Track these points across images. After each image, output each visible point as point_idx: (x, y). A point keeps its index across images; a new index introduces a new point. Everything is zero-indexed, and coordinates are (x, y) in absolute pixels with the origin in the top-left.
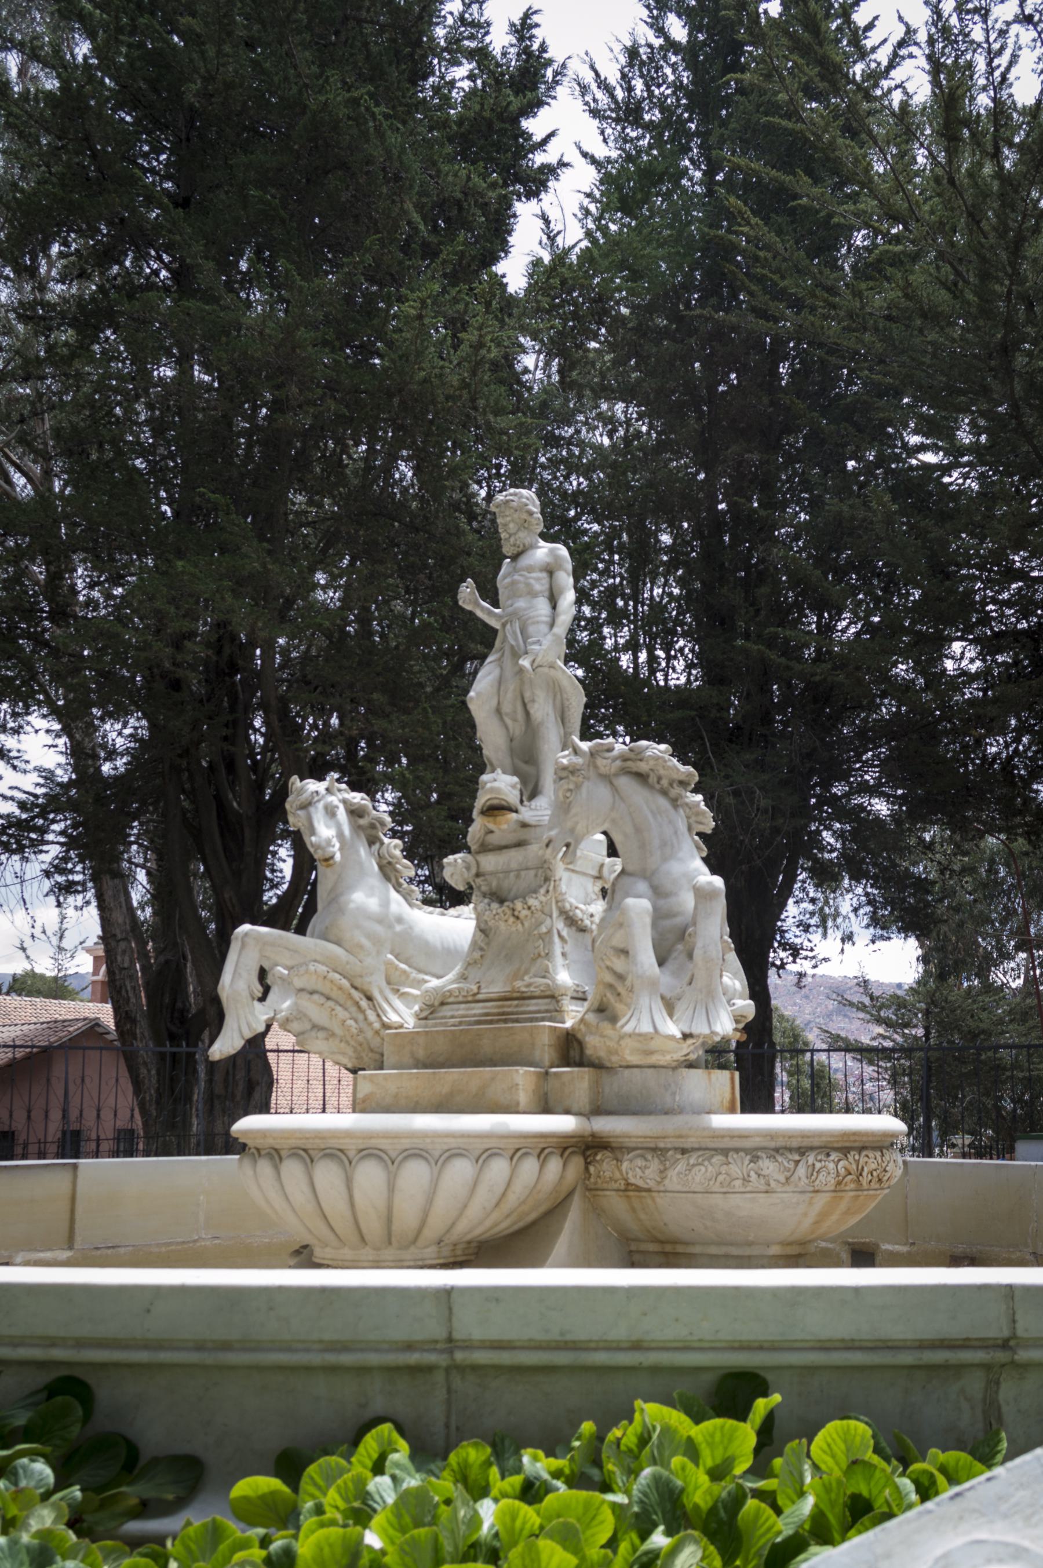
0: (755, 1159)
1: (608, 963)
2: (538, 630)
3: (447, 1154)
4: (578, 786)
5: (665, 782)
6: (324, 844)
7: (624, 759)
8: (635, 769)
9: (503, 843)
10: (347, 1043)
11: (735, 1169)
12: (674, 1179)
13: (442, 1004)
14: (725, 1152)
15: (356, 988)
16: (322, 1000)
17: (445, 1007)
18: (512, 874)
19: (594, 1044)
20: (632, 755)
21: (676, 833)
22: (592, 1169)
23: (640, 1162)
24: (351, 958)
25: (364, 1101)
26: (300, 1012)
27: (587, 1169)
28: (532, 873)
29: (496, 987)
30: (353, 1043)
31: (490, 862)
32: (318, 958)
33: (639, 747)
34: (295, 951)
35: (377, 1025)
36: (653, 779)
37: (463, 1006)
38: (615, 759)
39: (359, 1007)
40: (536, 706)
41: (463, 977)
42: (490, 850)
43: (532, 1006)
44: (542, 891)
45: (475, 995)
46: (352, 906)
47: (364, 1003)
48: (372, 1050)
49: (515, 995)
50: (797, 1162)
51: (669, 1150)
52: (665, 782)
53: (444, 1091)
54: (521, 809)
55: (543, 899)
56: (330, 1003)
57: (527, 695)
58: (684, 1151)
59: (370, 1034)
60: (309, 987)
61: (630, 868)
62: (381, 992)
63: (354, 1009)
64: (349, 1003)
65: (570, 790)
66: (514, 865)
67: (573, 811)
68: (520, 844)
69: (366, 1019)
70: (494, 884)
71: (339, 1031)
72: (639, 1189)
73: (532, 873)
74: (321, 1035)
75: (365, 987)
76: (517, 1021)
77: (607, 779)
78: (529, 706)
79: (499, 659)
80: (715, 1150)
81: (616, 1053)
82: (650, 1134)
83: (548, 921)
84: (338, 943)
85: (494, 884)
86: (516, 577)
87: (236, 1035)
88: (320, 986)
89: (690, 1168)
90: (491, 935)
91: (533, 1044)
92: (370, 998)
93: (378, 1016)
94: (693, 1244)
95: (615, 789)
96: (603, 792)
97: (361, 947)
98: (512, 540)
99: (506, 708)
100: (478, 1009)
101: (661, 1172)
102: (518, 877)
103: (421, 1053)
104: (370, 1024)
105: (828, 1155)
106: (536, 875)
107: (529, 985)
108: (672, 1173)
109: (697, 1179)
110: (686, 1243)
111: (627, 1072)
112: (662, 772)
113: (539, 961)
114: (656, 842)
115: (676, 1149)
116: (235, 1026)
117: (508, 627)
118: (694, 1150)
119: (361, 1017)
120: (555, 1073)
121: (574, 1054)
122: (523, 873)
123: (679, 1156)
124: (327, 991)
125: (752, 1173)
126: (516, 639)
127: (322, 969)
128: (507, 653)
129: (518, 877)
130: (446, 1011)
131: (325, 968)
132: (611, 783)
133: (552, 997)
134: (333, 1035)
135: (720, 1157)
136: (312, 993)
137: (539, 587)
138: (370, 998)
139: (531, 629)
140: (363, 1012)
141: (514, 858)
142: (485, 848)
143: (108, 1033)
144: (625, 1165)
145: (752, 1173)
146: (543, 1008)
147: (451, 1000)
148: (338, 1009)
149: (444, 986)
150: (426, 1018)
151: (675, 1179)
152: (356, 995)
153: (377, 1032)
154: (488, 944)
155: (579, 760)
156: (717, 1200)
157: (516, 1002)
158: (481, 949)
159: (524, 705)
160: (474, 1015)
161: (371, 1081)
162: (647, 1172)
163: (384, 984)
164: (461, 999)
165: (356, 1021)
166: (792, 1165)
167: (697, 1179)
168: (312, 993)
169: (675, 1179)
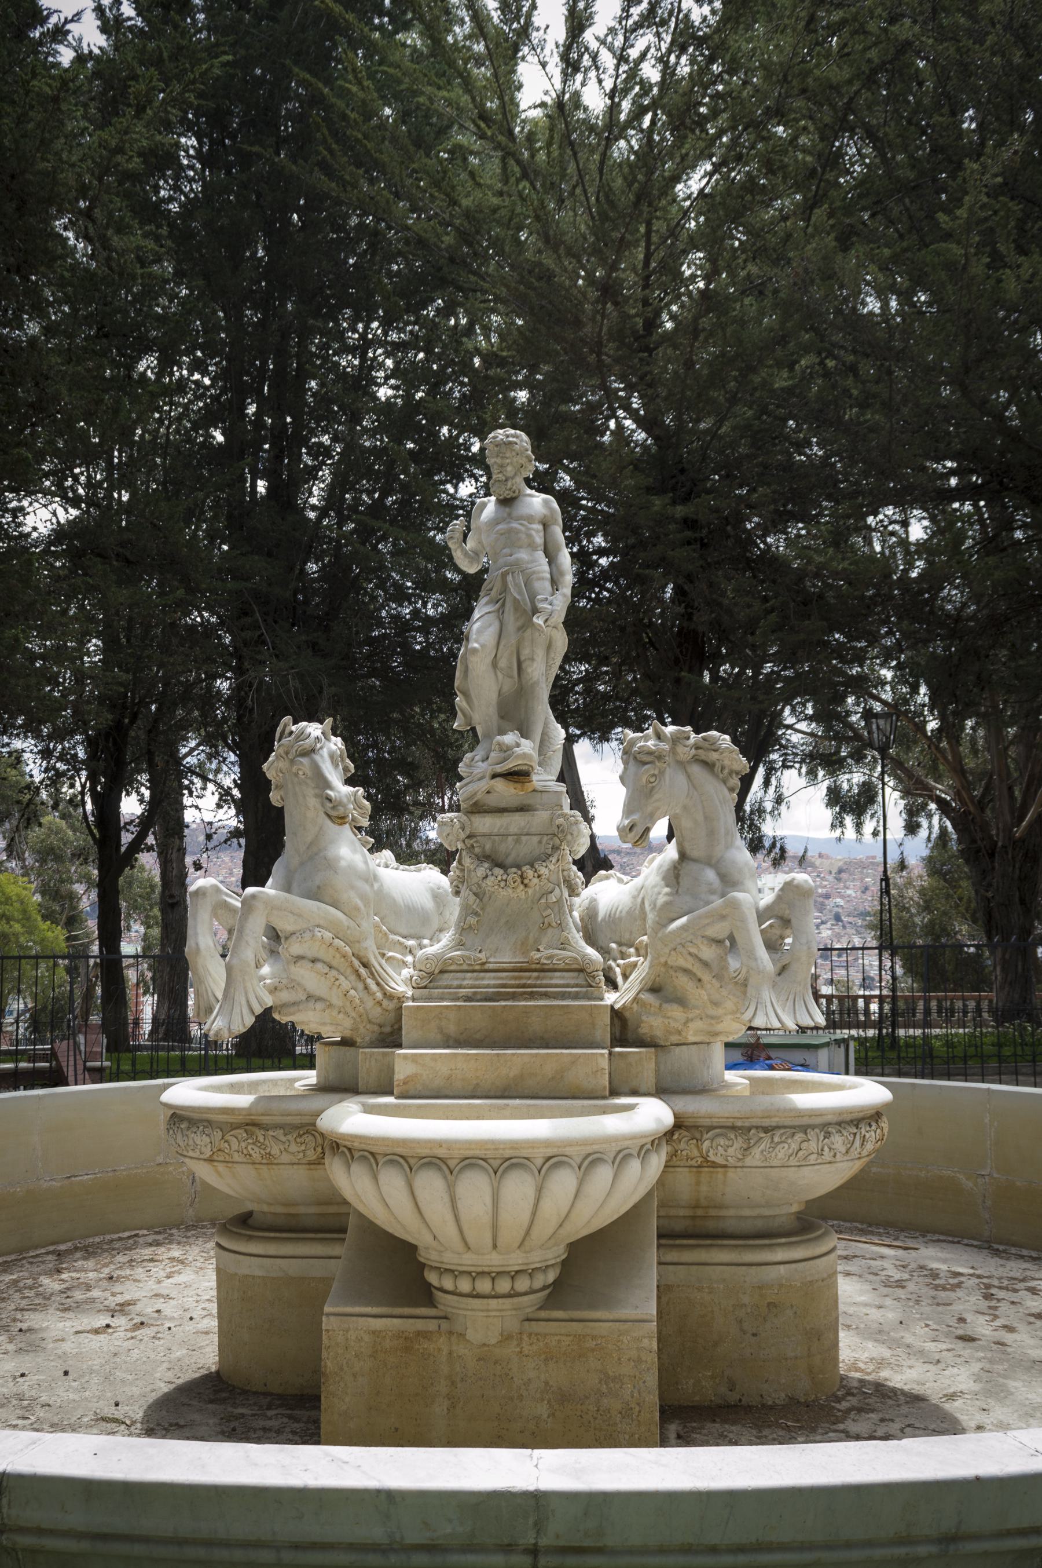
0: (827, 1135)
1: (693, 950)
2: (544, 586)
3: (621, 1156)
4: (662, 772)
5: (726, 771)
7: (697, 747)
8: (703, 758)
9: (503, 805)
10: (346, 1013)
11: (813, 1145)
12: (756, 1156)
13: (442, 972)
14: (805, 1129)
16: (326, 969)
17: (446, 975)
18: (510, 838)
19: (653, 1024)
20: (706, 745)
23: (722, 1141)
24: (352, 924)
25: (405, 1083)
26: (293, 980)
29: (507, 957)
30: (353, 1014)
31: (484, 824)
32: (322, 923)
33: (712, 736)
34: (300, 916)
35: (379, 995)
36: (717, 769)
37: (469, 975)
40: (535, 665)
41: (460, 944)
42: (486, 812)
43: (557, 979)
44: (554, 860)
45: (483, 964)
46: (343, 863)
47: (363, 971)
48: (370, 1022)
49: (534, 966)
51: (749, 1129)
52: (726, 771)
53: (511, 1075)
55: (552, 867)
56: (334, 973)
57: (525, 652)
58: (766, 1130)
59: (370, 1003)
60: (310, 954)
61: (694, 853)
63: (353, 977)
64: (349, 971)
65: (654, 775)
66: (513, 829)
67: (656, 796)
68: (522, 809)
70: (488, 847)
71: (337, 1001)
72: (714, 1165)
73: (536, 839)
74: (319, 1006)
75: (362, 954)
76: (546, 995)
77: (681, 764)
78: (524, 666)
80: (794, 1127)
81: (679, 1033)
82: (737, 1115)
83: (557, 890)
84: (335, 905)
85: (488, 847)
86: (515, 525)
87: (246, 1011)
88: (322, 954)
89: (774, 1146)
90: (486, 899)
91: (593, 1024)
92: (365, 965)
93: (378, 984)
94: (727, 1207)
96: (681, 779)
97: (357, 909)
98: (509, 484)
99: (503, 663)
100: (489, 980)
101: (746, 1150)
102: (518, 841)
103: (452, 1029)
106: (540, 842)
107: (550, 957)
108: (756, 1152)
109: (780, 1155)
110: (721, 1207)
111: (678, 1049)
112: (726, 762)
113: (550, 931)
114: (723, 831)
115: (757, 1128)
118: (778, 1127)
119: (360, 986)
120: (620, 1053)
122: (524, 838)
123: (762, 1135)
124: (328, 958)
125: (826, 1149)
126: (520, 593)
127: (328, 935)
129: (518, 841)
130: (447, 979)
133: (581, 971)
134: (331, 1006)
135: (802, 1135)
136: (314, 961)
137: (539, 540)
138: (365, 965)
139: (537, 585)
140: (364, 981)
141: (516, 822)
142: (477, 809)
144: (707, 1144)
145: (826, 1149)
146: (572, 982)
147: (452, 968)
148: (342, 978)
149: (443, 953)
150: (425, 987)
151: (757, 1156)
153: (380, 1003)
154: (482, 909)
155: (665, 746)
156: (791, 1173)
157: (535, 974)
158: (476, 914)
160: (488, 986)
162: (731, 1151)
164: (465, 967)
166: (851, 1138)
167: (780, 1155)
168: (314, 961)
169: (757, 1156)
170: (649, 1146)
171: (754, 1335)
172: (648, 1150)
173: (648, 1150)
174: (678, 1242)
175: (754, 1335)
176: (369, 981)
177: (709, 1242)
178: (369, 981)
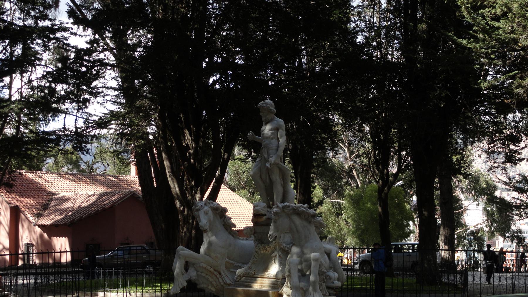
6: (203, 226)
15: (215, 270)
21: (310, 233)
35: (222, 284)
38: (290, 210)
45: (253, 275)
47: (218, 276)
55: (275, 244)
62: (224, 272)
63: (215, 278)
69: (219, 281)
104: (220, 283)
119: (217, 280)
131: (205, 265)
132: (289, 217)
138: (220, 274)
140: (218, 279)
143: (139, 198)
152: (216, 273)
159: (269, 176)
163: (225, 268)
165: (216, 282)
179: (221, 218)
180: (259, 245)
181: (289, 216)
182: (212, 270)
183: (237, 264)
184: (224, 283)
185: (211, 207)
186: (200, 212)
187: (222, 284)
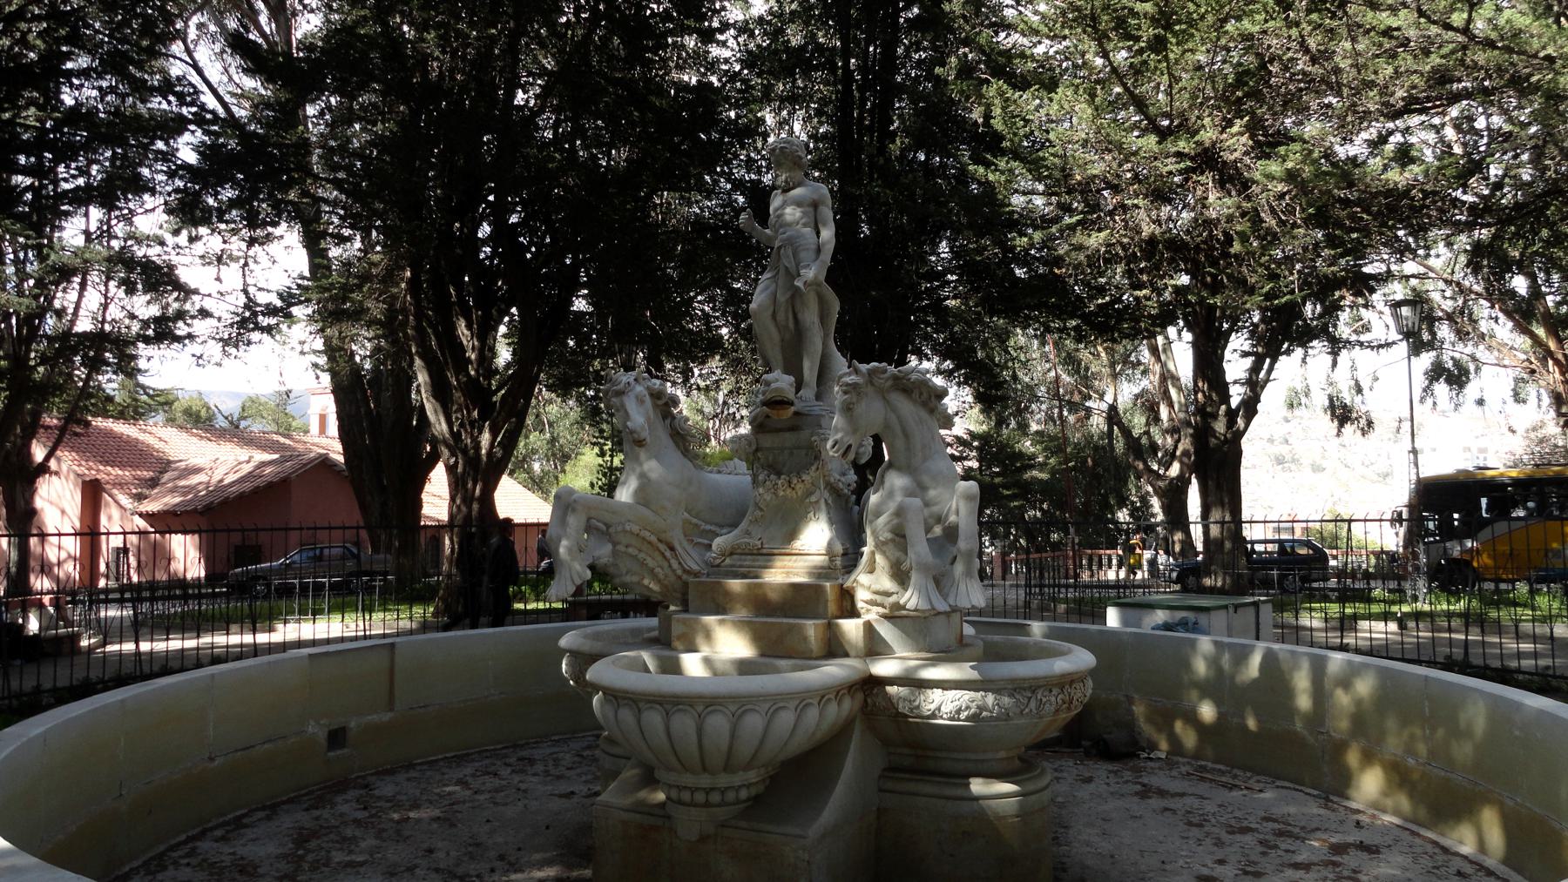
5: (925, 395)
6: (638, 429)
15: (660, 541)
22: (869, 700)
27: (865, 701)
28: (804, 452)
35: (679, 572)
38: (887, 379)
39: (664, 557)
44: (814, 468)
47: (668, 554)
50: (1030, 698)
54: (796, 401)
59: (672, 578)
63: (660, 558)
69: (670, 566)
73: (804, 452)
79: (774, 277)
87: (569, 583)
95: (887, 401)
104: (674, 571)
105: (1051, 691)
116: (568, 575)
117: (782, 251)
119: (665, 564)
121: (847, 604)
128: (782, 271)
129: (791, 454)
132: (884, 398)
138: (672, 549)
140: (668, 561)
141: (789, 439)
152: (662, 547)
161: (684, 624)
163: (682, 537)
165: (662, 568)
170: (832, 696)
171: (952, 855)
172: (829, 700)
173: (829, 700)
174: (897, 775)
175: (952, 855)
176: (673, 562)
177: (907, 776)
178: (673, 562)
179: (664, 418)
180: (772, 477)
181: (882, 393)
182: (653, 539)
183: (708, 527)
184: (685, 571)
185: (648, 388)
186: (625, 399)
187: (679, 572)
